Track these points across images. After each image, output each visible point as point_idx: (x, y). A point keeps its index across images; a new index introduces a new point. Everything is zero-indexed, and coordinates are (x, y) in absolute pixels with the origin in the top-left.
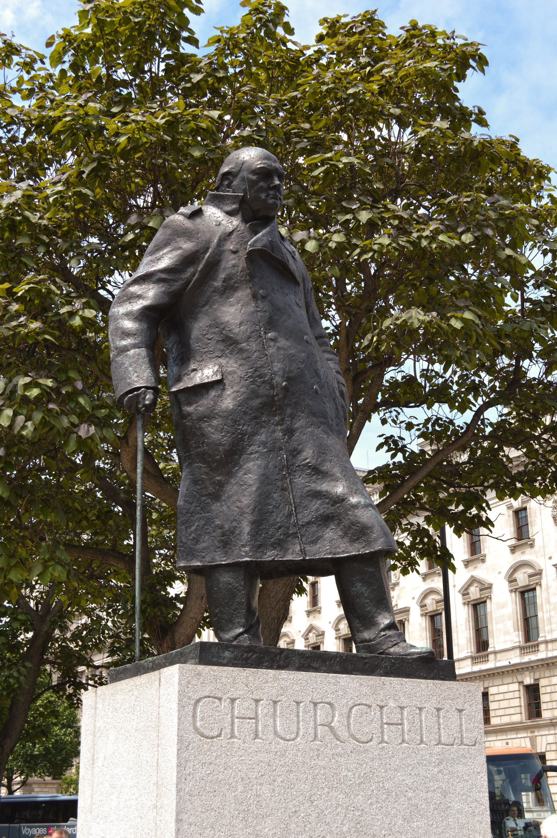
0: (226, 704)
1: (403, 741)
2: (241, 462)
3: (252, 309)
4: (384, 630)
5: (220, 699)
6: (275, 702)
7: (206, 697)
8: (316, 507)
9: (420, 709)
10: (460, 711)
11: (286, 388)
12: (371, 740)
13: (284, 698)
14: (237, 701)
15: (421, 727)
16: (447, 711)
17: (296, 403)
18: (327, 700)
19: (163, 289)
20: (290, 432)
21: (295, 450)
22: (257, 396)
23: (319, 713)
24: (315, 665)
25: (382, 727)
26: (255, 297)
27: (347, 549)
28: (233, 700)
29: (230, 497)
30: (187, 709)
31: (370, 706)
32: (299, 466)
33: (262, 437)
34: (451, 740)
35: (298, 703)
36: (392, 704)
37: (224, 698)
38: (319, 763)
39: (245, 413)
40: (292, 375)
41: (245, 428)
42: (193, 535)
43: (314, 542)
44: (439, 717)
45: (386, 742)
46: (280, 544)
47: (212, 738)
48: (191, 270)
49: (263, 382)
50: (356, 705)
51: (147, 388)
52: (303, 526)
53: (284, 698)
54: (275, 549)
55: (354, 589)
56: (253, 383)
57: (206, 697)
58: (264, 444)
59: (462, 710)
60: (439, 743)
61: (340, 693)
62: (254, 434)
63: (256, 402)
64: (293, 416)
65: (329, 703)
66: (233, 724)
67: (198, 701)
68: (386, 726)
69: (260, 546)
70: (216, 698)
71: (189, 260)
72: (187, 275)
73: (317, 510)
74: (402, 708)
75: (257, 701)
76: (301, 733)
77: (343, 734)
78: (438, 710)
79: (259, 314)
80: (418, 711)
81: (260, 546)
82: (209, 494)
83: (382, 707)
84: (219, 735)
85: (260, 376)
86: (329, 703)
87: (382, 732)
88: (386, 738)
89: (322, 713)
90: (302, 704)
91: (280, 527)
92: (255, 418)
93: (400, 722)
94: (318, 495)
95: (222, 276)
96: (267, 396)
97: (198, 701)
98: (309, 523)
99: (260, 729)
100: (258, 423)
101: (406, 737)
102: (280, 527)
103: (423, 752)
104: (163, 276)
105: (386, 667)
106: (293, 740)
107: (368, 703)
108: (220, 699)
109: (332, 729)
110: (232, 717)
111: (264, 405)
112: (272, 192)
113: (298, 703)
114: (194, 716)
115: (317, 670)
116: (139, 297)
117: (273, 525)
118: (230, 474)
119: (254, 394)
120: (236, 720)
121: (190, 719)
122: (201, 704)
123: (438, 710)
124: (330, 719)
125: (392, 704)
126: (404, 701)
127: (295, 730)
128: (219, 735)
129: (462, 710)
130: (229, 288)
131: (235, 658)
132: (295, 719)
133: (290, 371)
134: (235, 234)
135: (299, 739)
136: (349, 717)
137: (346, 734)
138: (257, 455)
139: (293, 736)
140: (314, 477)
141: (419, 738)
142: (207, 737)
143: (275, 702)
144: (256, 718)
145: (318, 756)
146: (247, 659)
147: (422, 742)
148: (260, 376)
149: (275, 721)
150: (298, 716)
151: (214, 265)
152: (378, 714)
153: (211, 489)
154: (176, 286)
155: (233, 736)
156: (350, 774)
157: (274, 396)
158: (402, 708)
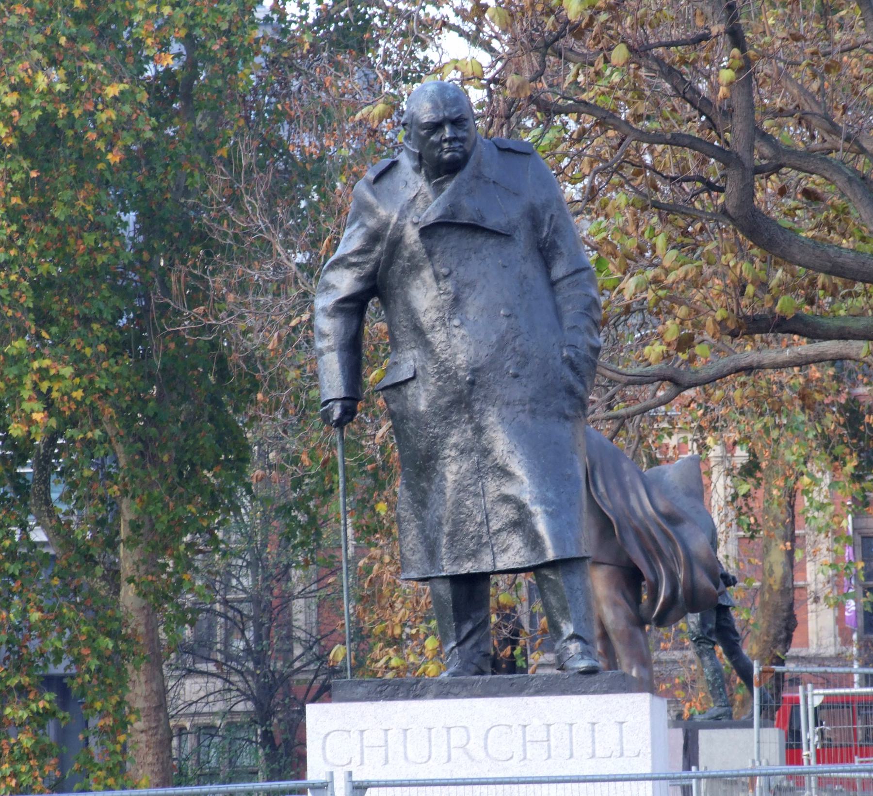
0: (355, 735)
2: (438, 468)
3: (435, 293)
4: (565, 641)
6: (406, 730)
8: (507, 513)
9: (571, 725)
11: (472, 383)
15: (571, 742)
17: (485, 396)
19: (355, 275)
20: (479, 430)
21: (486, 450)
22: (445, 394)
24: (455, 690)
25: (524, 745)
26: (437, 277)
28: (362, 732)
29: (432, 505)
31: (510, 727)
33: (453, 440)
36: (536, 722)
39: (435, 414)
40: (477, 366)
41: (436, 430)
43: (504, 551)
44: (593, 731)
46: (474, 555)
48: (378, 248)
49: (449, 377)
52: (494, 534)
54: (470, 560)
56: (439, 379)
58: (455, 446)
59: (622, 723)
60: (593, 756)
62: (447, 435)
63: (443, 401)
64: (482, 412)
66: (362, 753)
69: (456, 558)
71: (374, 238)
72: (374, 255)
73: (507, 516)
74: (549, 726)
75: (386, 730)
76: (433, 757)
78: (594, 724)
79: (444, 297)
80: (567, 727)
81: (456, 558)
85: (445, 371)
87: (525, 751)
88: (528, 756)
91: (473, 538)
92: (445, 418)
94: (506, 499)
95: (406, 254)
96: (454, 393)
98: (499, 531)
99: (390, 755)
100: (449, 423)
101: (553, 753)
102: (473, 538)
104: (353, 260)
105: (536, 686)
110: (362, 747)
111: (452, 404)
113: (430, 729)
114: (324, 748)
115: (457, 696)
117: (467, 535)
118: (429, 480)
119: (442, 391)
120: (365, 749)
121: (320, 752)
123: (594, 724)
124: (464, 742)
125: (536, 722)
129: (622, 723)
130: (415, 268)
131: (369, 693)
132: (427, 745)
133: (476, 362)
134: (420, 198)
136: (486, 738)
137: (482, 755)
138: (449, 460)
139: (425, 759)
140: (503, 480)
141: (568, 753)
143: (406, 730)
146: (381, 692)
147: (571, 756)
148: (445, 371)
149: (405, 747)
150: (430, 741)
151: (396, 243)
152: (520, 733)
153: (419, 497)
154: (368, 267)
157: (462, 391)
158: (549, 726)
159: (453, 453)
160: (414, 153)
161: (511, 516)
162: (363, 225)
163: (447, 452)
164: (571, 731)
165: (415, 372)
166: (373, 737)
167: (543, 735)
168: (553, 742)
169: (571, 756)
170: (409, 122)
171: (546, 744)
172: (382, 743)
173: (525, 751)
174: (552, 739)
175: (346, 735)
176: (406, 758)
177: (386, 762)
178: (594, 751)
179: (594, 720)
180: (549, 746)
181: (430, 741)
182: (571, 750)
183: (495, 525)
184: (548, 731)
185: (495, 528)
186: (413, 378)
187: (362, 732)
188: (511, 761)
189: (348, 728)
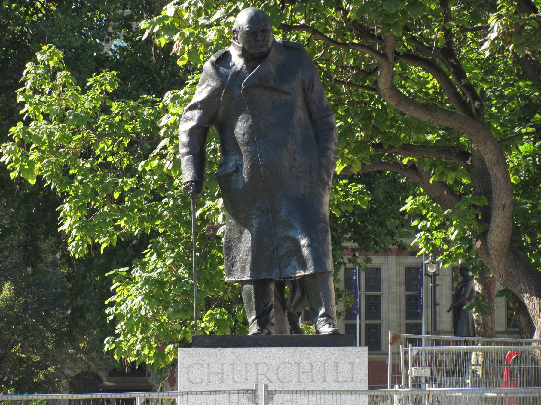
0: (205, 366)
1: (313, 381)
12: (291, 381)
13: (237, 362)
15: (324, 373)
23: (259, 368)
25: (299, 373)
28: (209, 365)
30: (183, 370)
35: (247, 364)
43: (286, 267)
44: (337, 366)
47: (198, 383)
53: (237, 362)
61: (272, 357)
80: (322, 364)
87: (299, 377)
114: (188, 373)
116: (191, 119)
125: (305, 361)
127: (244, 377)
132: (244, 372)
141: (322, 379)
147: (325, 381)
149: (233, 373)
150: (246, 370)
152: (296, 367)
159: (258, 213)
160: (240, 47)
162: (208, 85)
163: (254, 212)
164: (324, 366)
165: (237, 168)
166: (215, 368)
167: (308, 369)
169: (325, 381)
170: (237, 29)
171: (310, 374)
172: (219, 371)
173: (299, 377)
174: (314, 371)
175: (200, 366)
176: (234, 380)
178: (337, 377)
180: (312, 374)
181: (246, 370)
182: (325, 376)
185: (281, 254)
189: (201, 362)
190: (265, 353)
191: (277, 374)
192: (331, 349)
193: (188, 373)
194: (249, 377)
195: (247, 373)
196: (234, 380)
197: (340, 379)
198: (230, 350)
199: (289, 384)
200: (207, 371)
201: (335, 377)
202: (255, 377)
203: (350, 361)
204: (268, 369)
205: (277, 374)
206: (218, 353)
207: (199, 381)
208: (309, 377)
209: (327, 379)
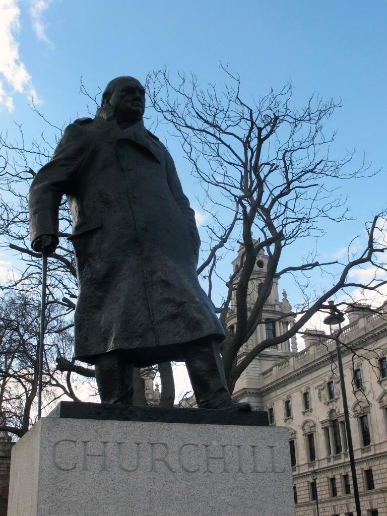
4: (216, 393)
5: (75, 442)
6: (120, 444)
7: (63, 440)
9: (238, 447)
10: (271, 447)
14: (89, 443)
16: (261, 448)
18: (161, 442)
27: (188, 337)
31: (197, 446)
32: (155, 282)
34: (264, 469)
36: (215, 443)
37: (78, 441)
38: (155, 488)
42: (84, 335)
45: (211, 472)
47: (68, 470)
50: (185, 445)
51: (48, 235)
55: (195, 365)
57: (63, 440)
61: (173, 436)
65: (165, 445)
66: (85, 460)
67: (58, 443)
68: (210, 460)
70: (71, 441)
71: (80, 151)
74: (224, 446)
75: (104, 443)
77: (176, 466)
78: (253, 447)
80: (236, 448)
82: (95, 306)
83: (207, 446)
84: (74, 468)
86: (165, 445)
87: (208, 465)
89: (159, 452)
90: (141, 445)
91: (141, 325)
93: (221, 456)
94: (167, 301)
97: (58, 443)
98: (162, 321)
102: (141, 325)
103: (241, 478)
106: (134, 471)
107: (195, 443)
108: (75, 442)
109: (167, 464)
112: (136, 102)
114: (54, 455)
122: (59, 445)
126: (225, 441)
127: (135, 463)
128: (74, 468)
129: (273, 447)
135: (138, 470)
139: (134, 468)
141: (237, 468)
142: (64, 470)
144: (104, 455)
145: (154, 482)
146: (99, 413)
147: (240, 470)
152: (204, 451)
155: (85, 469)
156: (180, 496)
161: (171, 311)
166: (94, 448)
168: (228, 459)
169: (240, 470)
173: (208, 465)
177: (104, 468)
179: (254, 444)
183: (158, 317)
184: (224, 450)
186: (100, 228)
187: (85, 443)
188: (198, 472)
189: (74, 439)
190: (164, 429)
191: (180, 460)
192: (247, 428)
193: (54, 455)
194: (142, 464)
195: (139, 458)
196: (121, 467)
197: (259, 469)
198: (117, 423)
199: (195, 475)
200: (83, 453)
201: (252, 467)
202: (151, 465)
203: (269, 445)
204: (168, 453)
205: (180, 460)
206: (100, 427)
207: (70, 468)
208: (220, 466)
209: (243, 469)
